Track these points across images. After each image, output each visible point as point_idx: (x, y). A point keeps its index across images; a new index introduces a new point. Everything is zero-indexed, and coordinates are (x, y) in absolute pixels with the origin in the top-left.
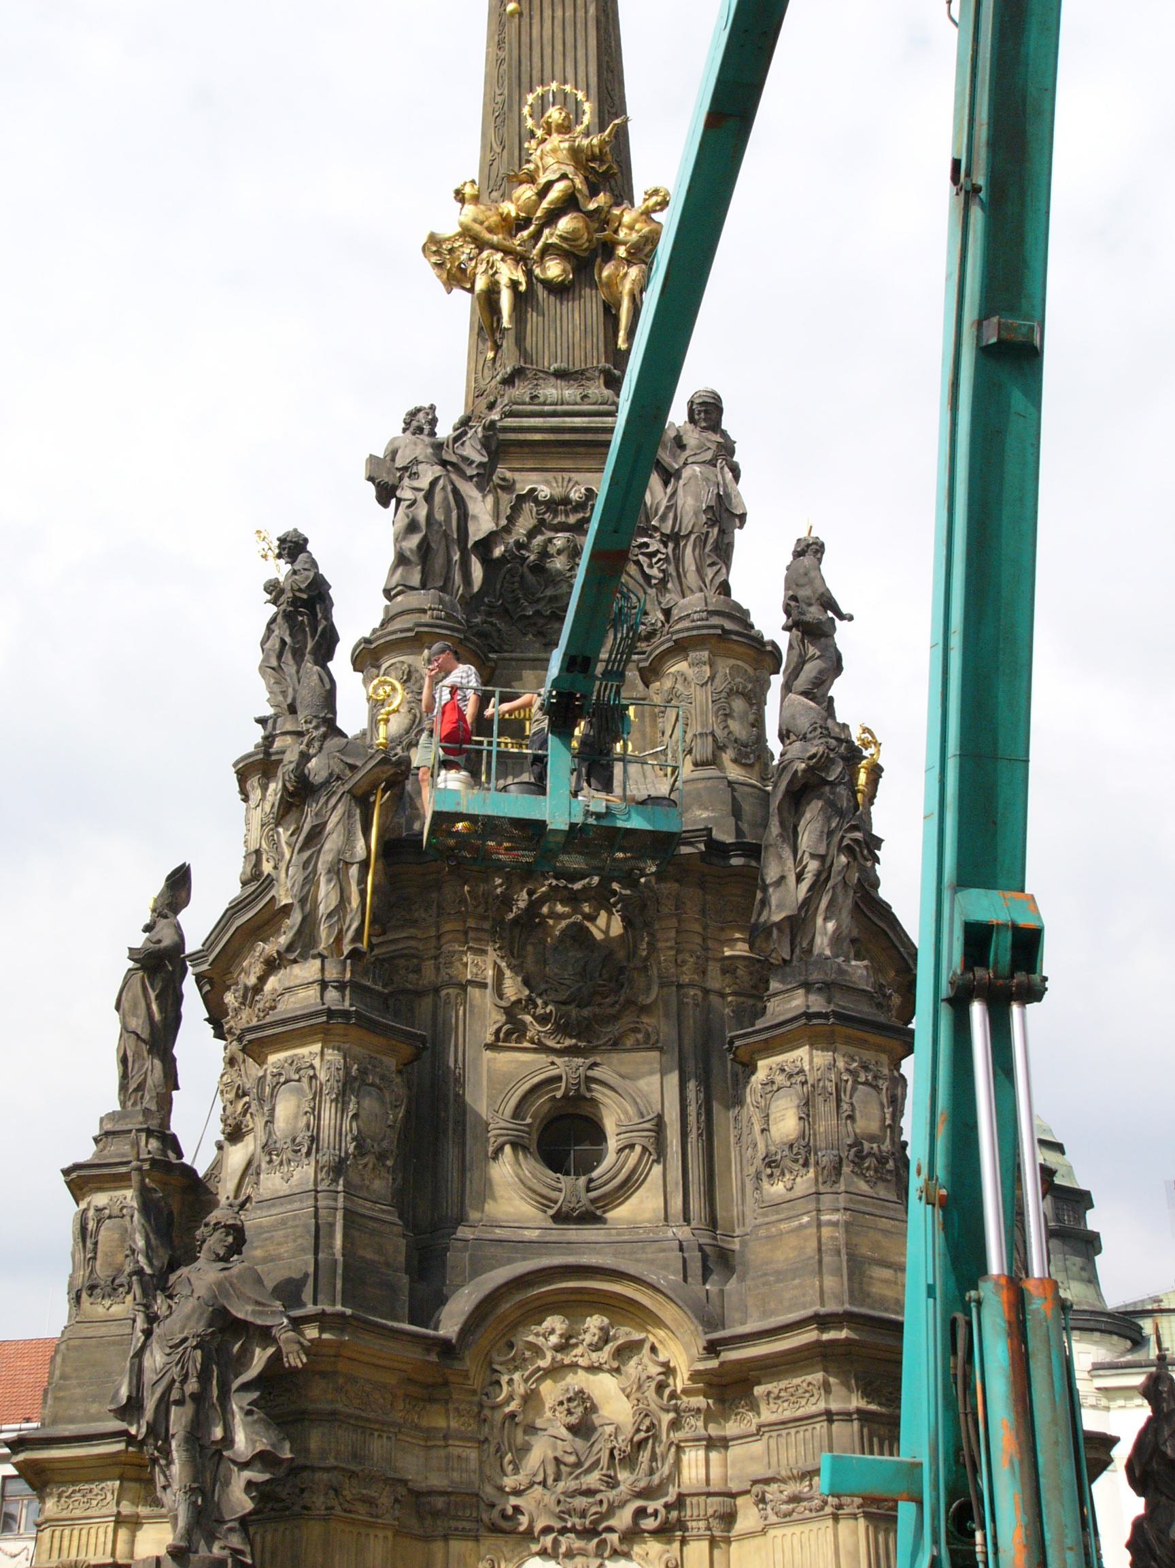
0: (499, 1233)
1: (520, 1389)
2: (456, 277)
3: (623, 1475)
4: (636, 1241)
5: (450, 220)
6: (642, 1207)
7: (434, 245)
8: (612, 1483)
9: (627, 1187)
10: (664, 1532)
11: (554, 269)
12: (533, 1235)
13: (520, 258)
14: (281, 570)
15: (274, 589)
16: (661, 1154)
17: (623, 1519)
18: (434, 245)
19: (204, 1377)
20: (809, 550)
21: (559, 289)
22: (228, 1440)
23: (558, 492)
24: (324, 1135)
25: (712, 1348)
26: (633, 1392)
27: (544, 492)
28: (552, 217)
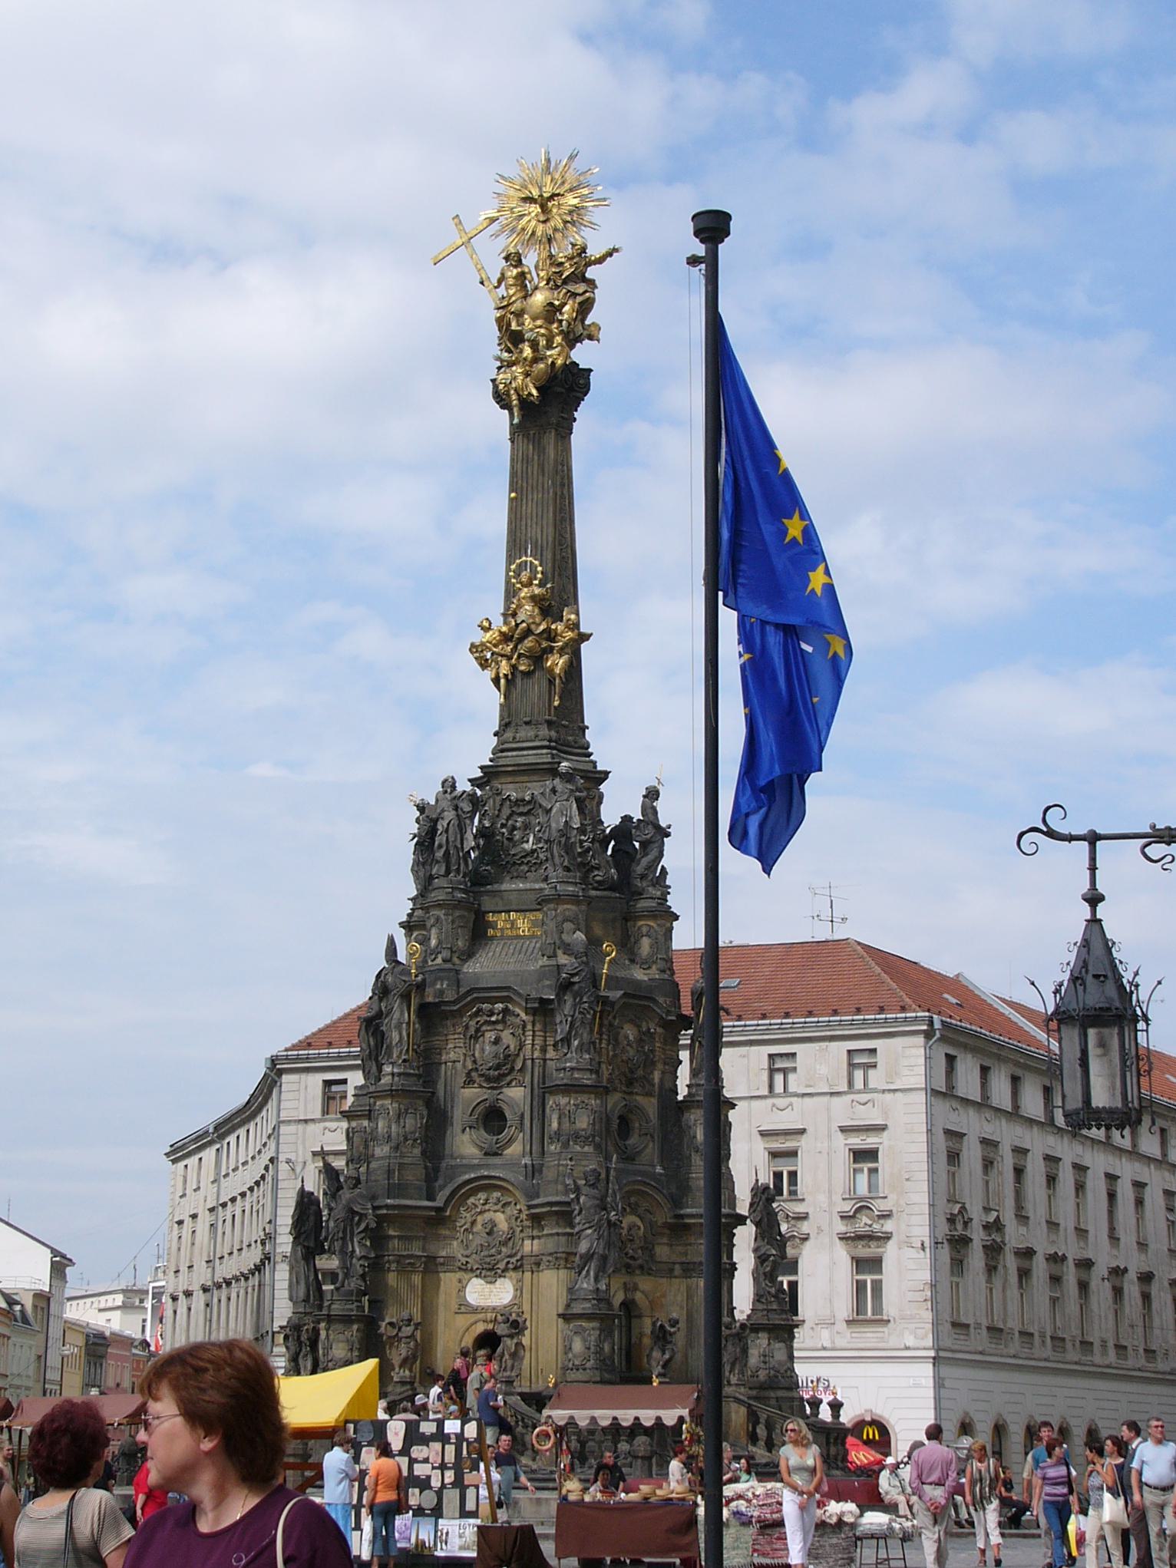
0: (464, 1162)
1: (470, 1220)
2: (484, 664)
3: (504, 1250)
4: (513, 1165)
6: (515, 1149)
7: (473, 648)
8: (500, 1253)
9: (510, 1141)
10: (515, 1269)
12: (476, 1162)
13: (509, 658)
16: (522, 1130)
17: (502, 1265)
18: (473, 648)
19: (344, 1231)
20: (652, 794)
21: (527, 674)
22: (353, 1251)
23: (520, 796)
24: (394, 1135)
25: (530, 1207)
26: (508, 1220)
28: (521, 640)
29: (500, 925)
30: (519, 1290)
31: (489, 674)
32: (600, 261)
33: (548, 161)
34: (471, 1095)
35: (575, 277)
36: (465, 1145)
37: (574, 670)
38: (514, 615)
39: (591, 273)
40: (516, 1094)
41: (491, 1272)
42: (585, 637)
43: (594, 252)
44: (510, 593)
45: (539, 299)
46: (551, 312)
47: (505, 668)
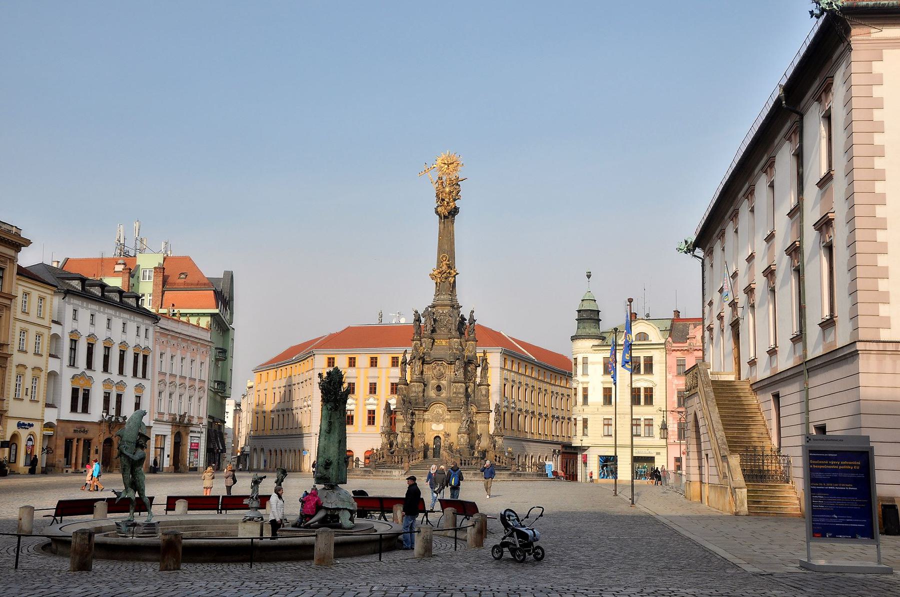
5: (432, 272)
20: (472, 312)
31: (434, 282)
34: (434, 382)
36: (432, 393)
37: (454, 282)
40: (444, 382)
44: (439, 262)
45: (447, 190)
46: (451, 192)
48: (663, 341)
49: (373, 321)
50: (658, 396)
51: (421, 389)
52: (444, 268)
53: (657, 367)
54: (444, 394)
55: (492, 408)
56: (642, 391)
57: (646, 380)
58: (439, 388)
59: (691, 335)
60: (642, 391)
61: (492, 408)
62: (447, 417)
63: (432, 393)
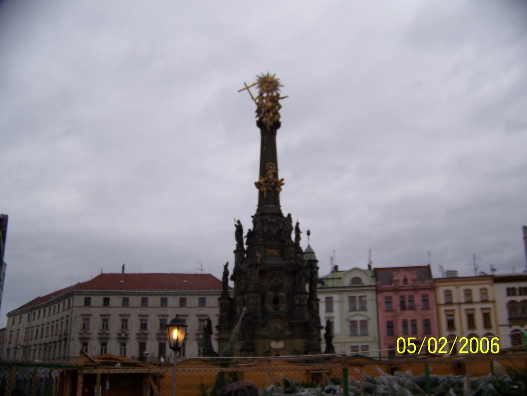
11: (270, 189)
13: (267, 187)
14: (237, 224)
15: (236, 225)
20: (298, 224)
21: (270, 191)
27: (270, 220)
29: (269, 252)
30: (285, 344)
32: (283, 98)
33: (268, 75)
34: (270, 294)
35: (275, 100)
36: (270, 307)
38: (268, 176)
39: (280, 102)
40: (282, 294)
41: (277, 339)
42: (283, 184)
43: (281, 96)
46: (273, 107)
47: (265, 189)
48: (373, 283)
49: (118, 270)
50: (372, 327)
51: (259, 301)
52: (271, 177)
53: (371, 305)
54: (283, 307)
55: (323, 323)
56: (359, 324)
57: (362, 315)
58: (276, 301)
59: (395, 278)
60: (359, 324)
61: (323, 323)
62: (288, 333)
63: (270, 307)
